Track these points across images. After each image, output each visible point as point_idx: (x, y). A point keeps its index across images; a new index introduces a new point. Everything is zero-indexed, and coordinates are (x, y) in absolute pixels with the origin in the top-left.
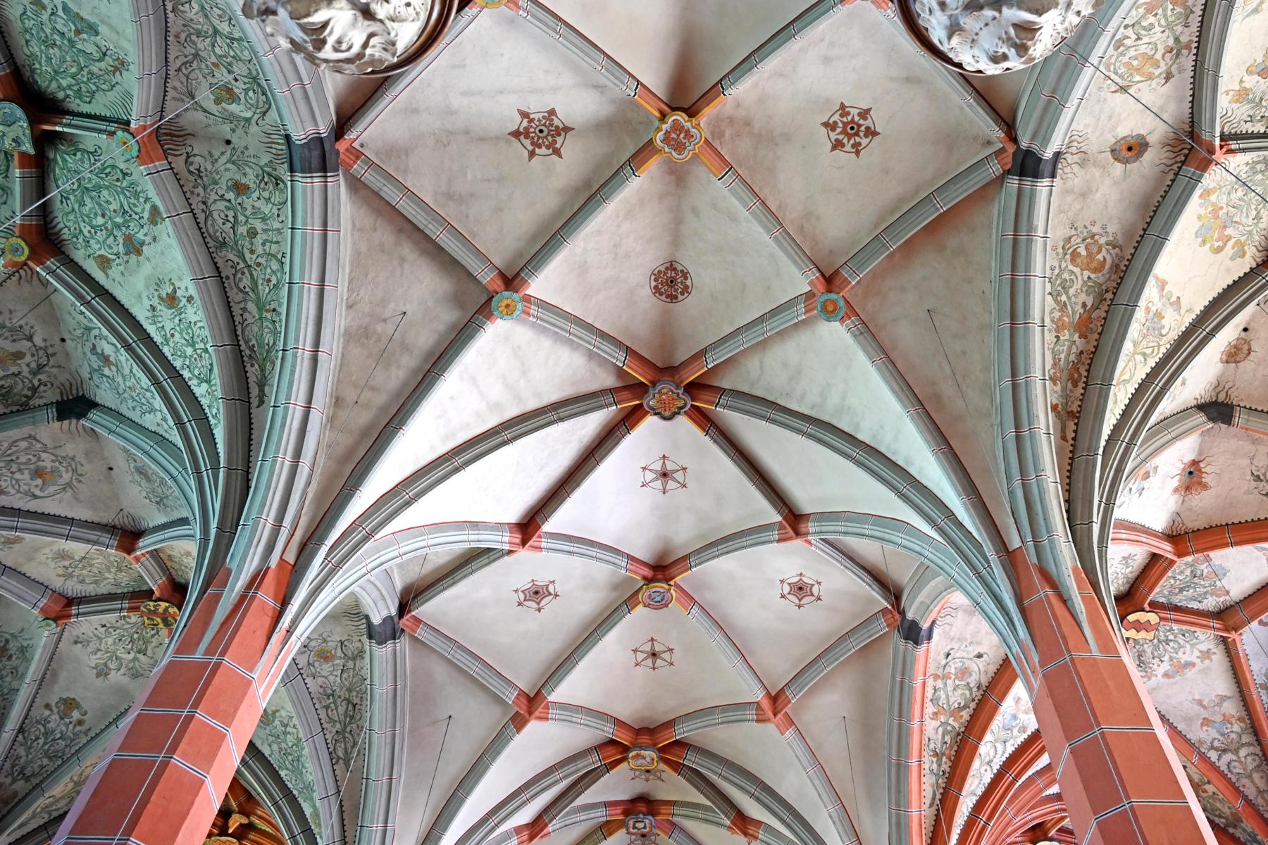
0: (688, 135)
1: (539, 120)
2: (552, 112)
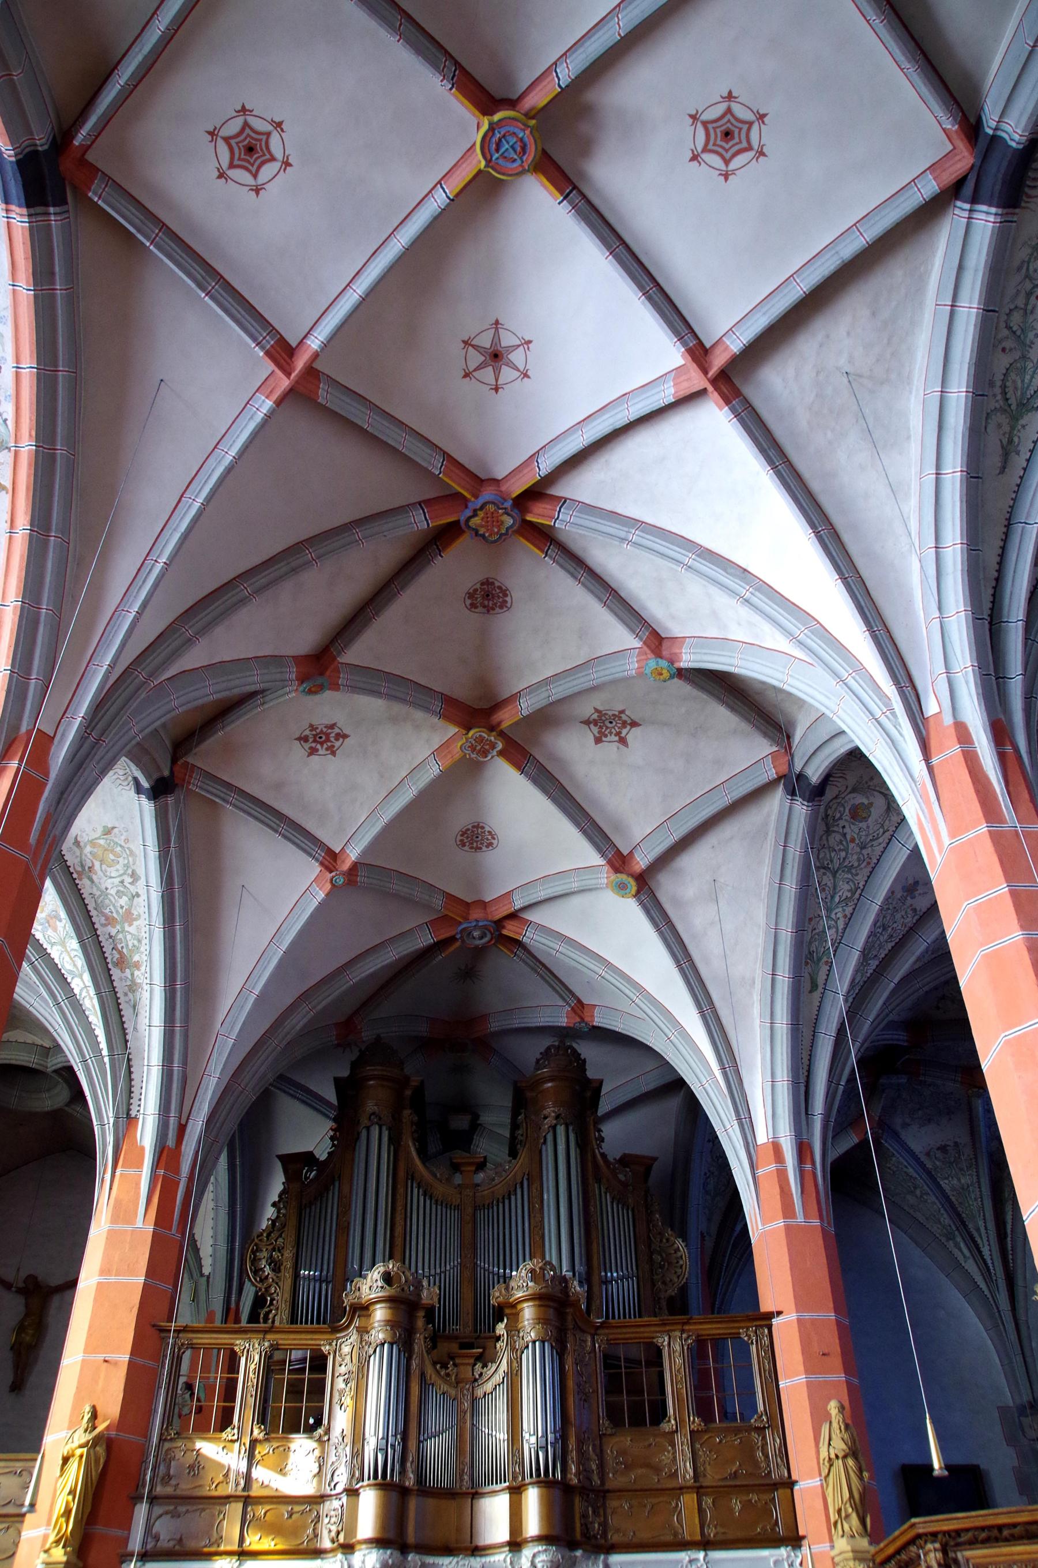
0: (473, 749)
1: (611, 733)
2: (598, 741)
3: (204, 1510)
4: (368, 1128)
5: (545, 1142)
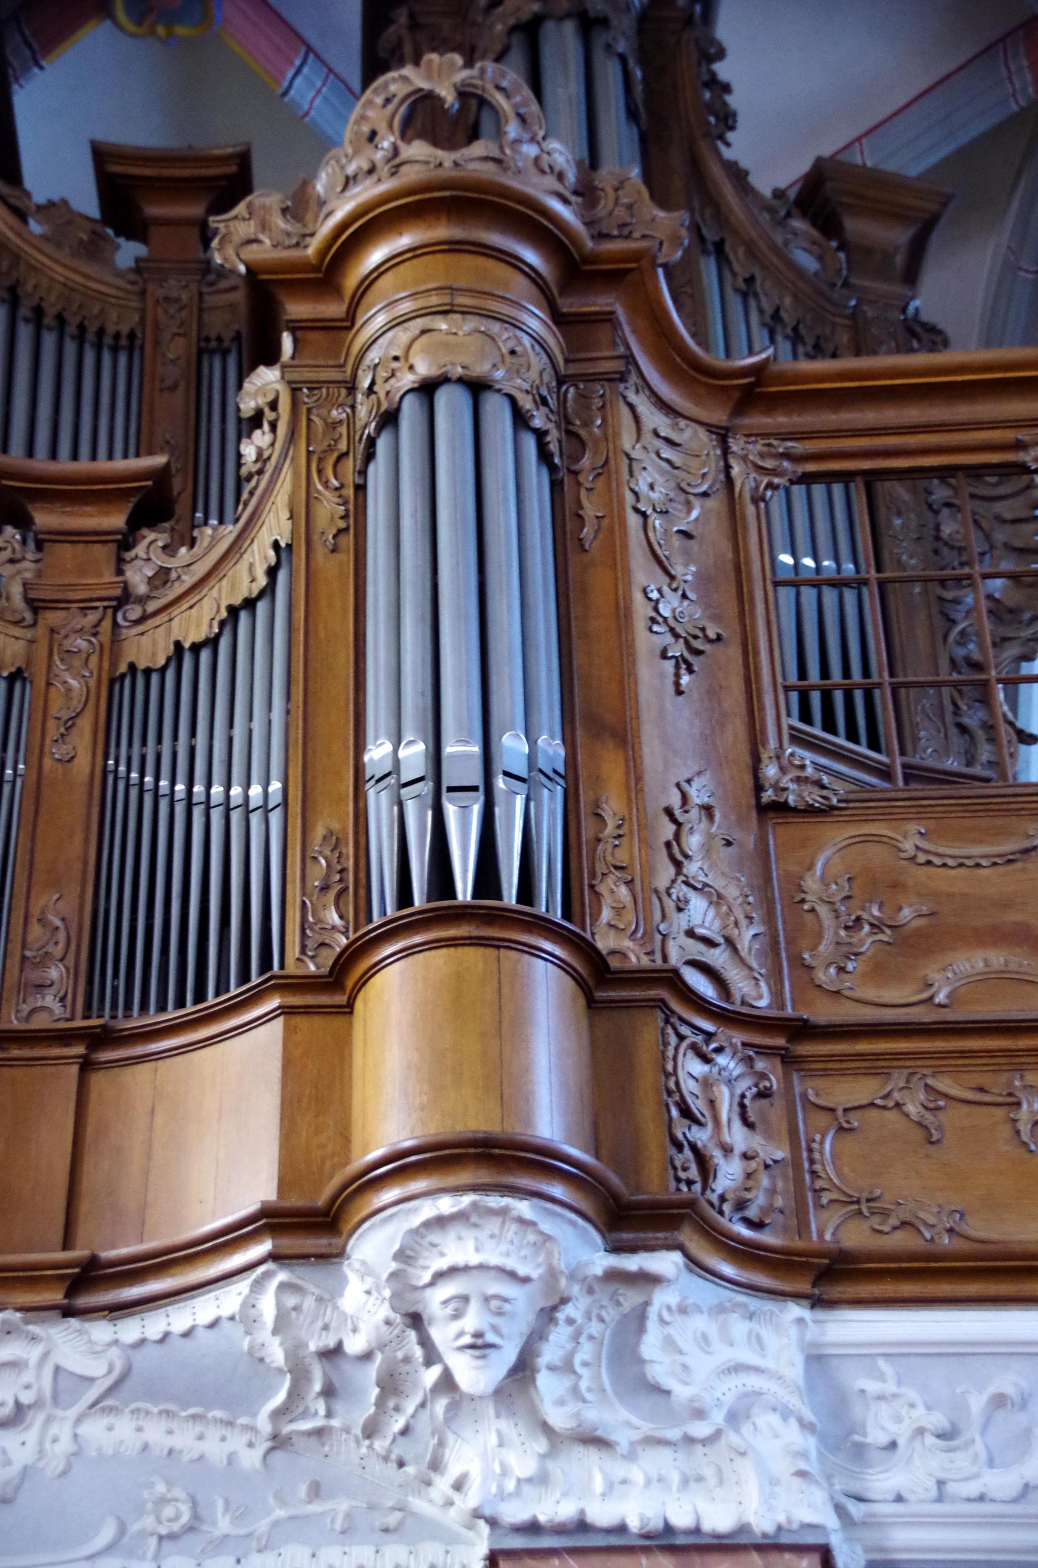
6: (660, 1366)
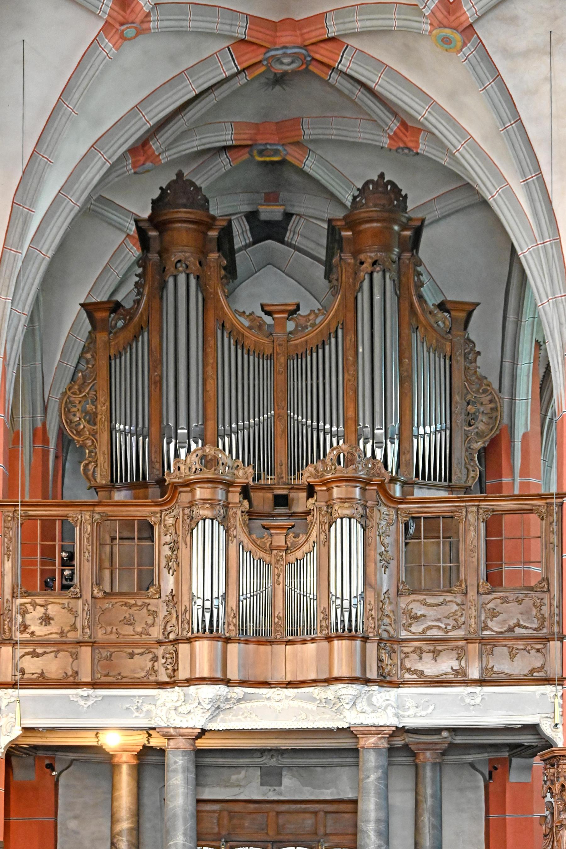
3: (58, 651)
4: (175, 277)
5: (361, 287)
6: (375, 703)
